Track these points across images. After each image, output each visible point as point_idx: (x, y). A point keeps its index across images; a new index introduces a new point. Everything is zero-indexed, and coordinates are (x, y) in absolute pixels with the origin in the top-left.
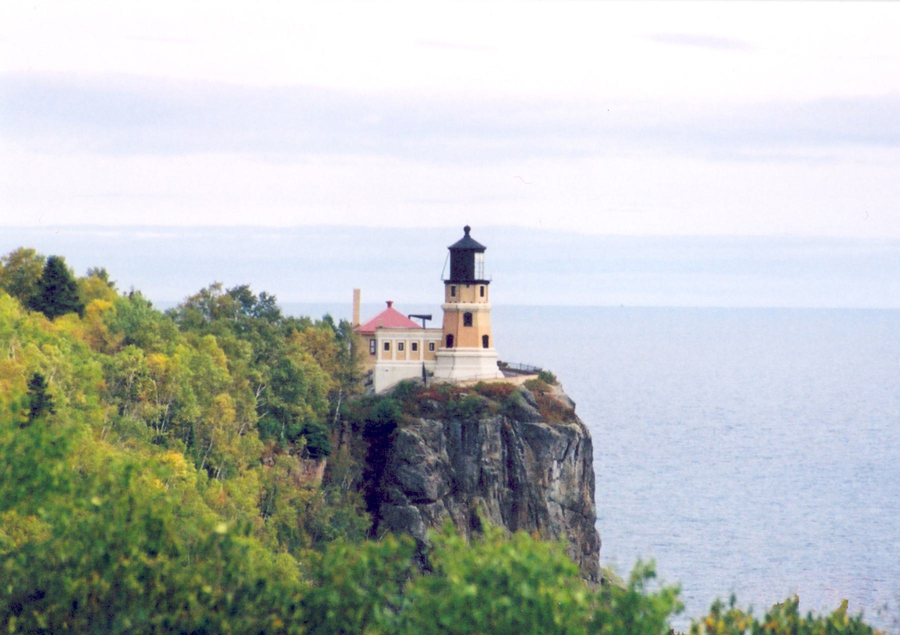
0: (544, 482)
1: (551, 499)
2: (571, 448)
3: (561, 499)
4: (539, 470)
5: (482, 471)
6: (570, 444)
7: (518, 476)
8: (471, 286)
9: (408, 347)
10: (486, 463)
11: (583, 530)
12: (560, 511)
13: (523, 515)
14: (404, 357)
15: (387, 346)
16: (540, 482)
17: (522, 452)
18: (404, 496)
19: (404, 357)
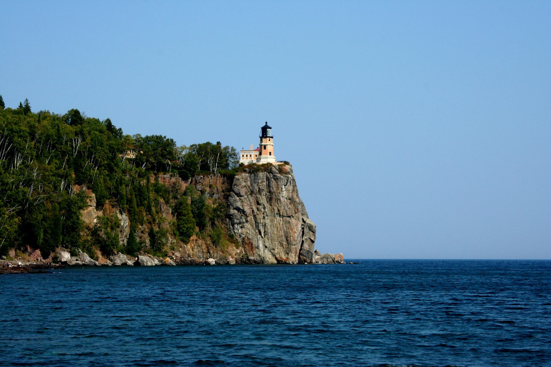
1: (282, 197)
3: (286, 197)
4: (278, 188)
5: (259, 188)
6: (287, 181)
11: (294, 206)
13: (274, 201)
15: (243, 156)
16: (278, 191)
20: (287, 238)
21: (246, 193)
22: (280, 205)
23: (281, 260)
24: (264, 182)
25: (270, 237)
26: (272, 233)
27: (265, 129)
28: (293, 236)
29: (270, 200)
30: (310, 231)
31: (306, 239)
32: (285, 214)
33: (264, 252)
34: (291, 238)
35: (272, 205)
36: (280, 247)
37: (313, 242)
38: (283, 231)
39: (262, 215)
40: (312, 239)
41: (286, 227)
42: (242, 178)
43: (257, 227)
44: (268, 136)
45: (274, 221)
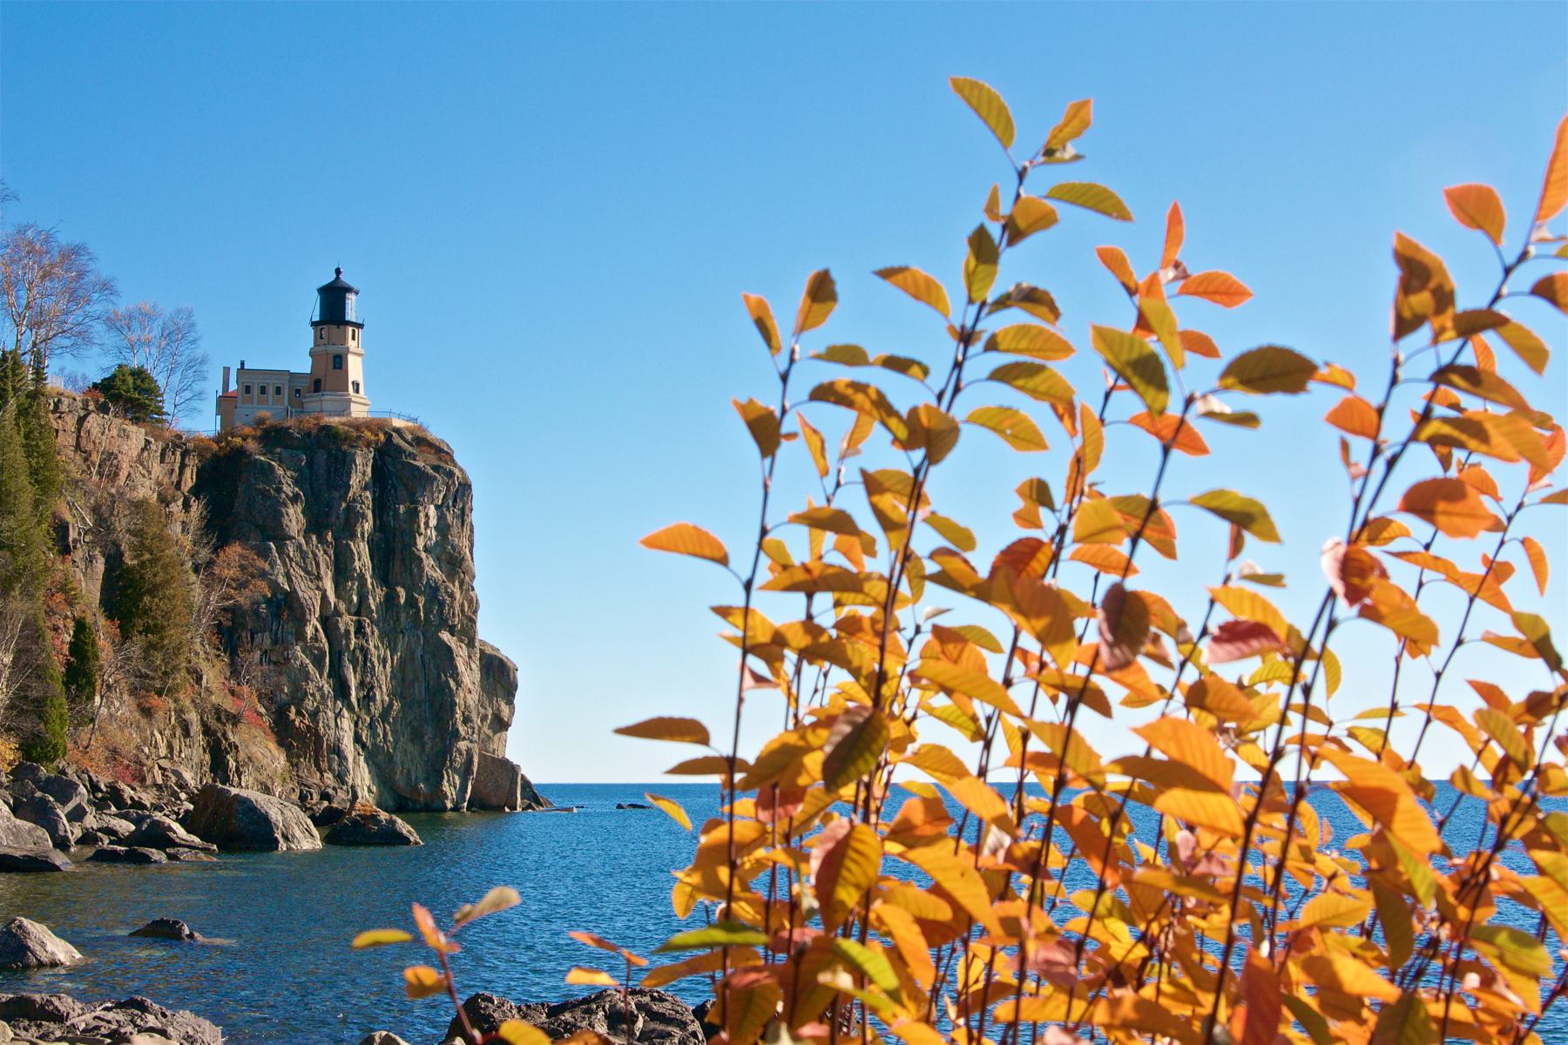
9: (271, 391)
17: (396, 492)
27: (334, 297)
36: (410, 748)
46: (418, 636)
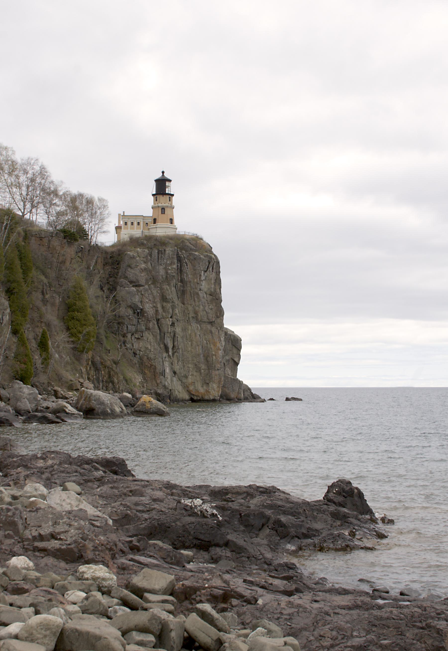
0: (197, 280)
2: (210, 265)
3: (206, 290)
5: (167, 273)
6: (209, 263)
7: (185, 277)
8: (164, 196)
9: (135, 224)
10: (169, 270)
11: (216, 306)
12: (205, 296)
13: (187, 296)
14: (134, 228)
15: (126, 224)
16: (195, 281)
17: (187, 266)
18: (128, 283)
19: (134, 228)
20: (206, 358)
21: (147, 282)
22: (197, 303)
23: (197, 394)
24: (174, 264)
25: (181, 356)
26: (184, 350)
28: (216, 355)
29: (182, 294)
30: (234, 347)
31: (228, 361)
32: (205, 319)
33: (172, 381)
34: (214, 357)
35: (185, 302)
36: (195, 374)
37: (237, 364)
38: (200, 347)
39: (171, 319)
40: (236, 360)
41: (206, 339)
42: (139, 256)
43: (162, 338)
44: (167, 192)
45: (188, 330)
46: (198, 327)
